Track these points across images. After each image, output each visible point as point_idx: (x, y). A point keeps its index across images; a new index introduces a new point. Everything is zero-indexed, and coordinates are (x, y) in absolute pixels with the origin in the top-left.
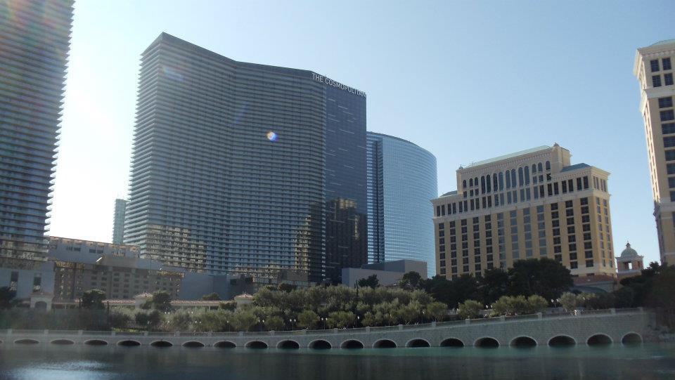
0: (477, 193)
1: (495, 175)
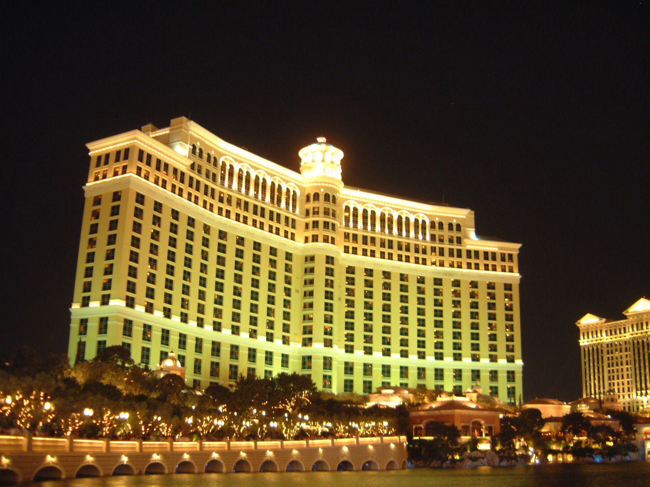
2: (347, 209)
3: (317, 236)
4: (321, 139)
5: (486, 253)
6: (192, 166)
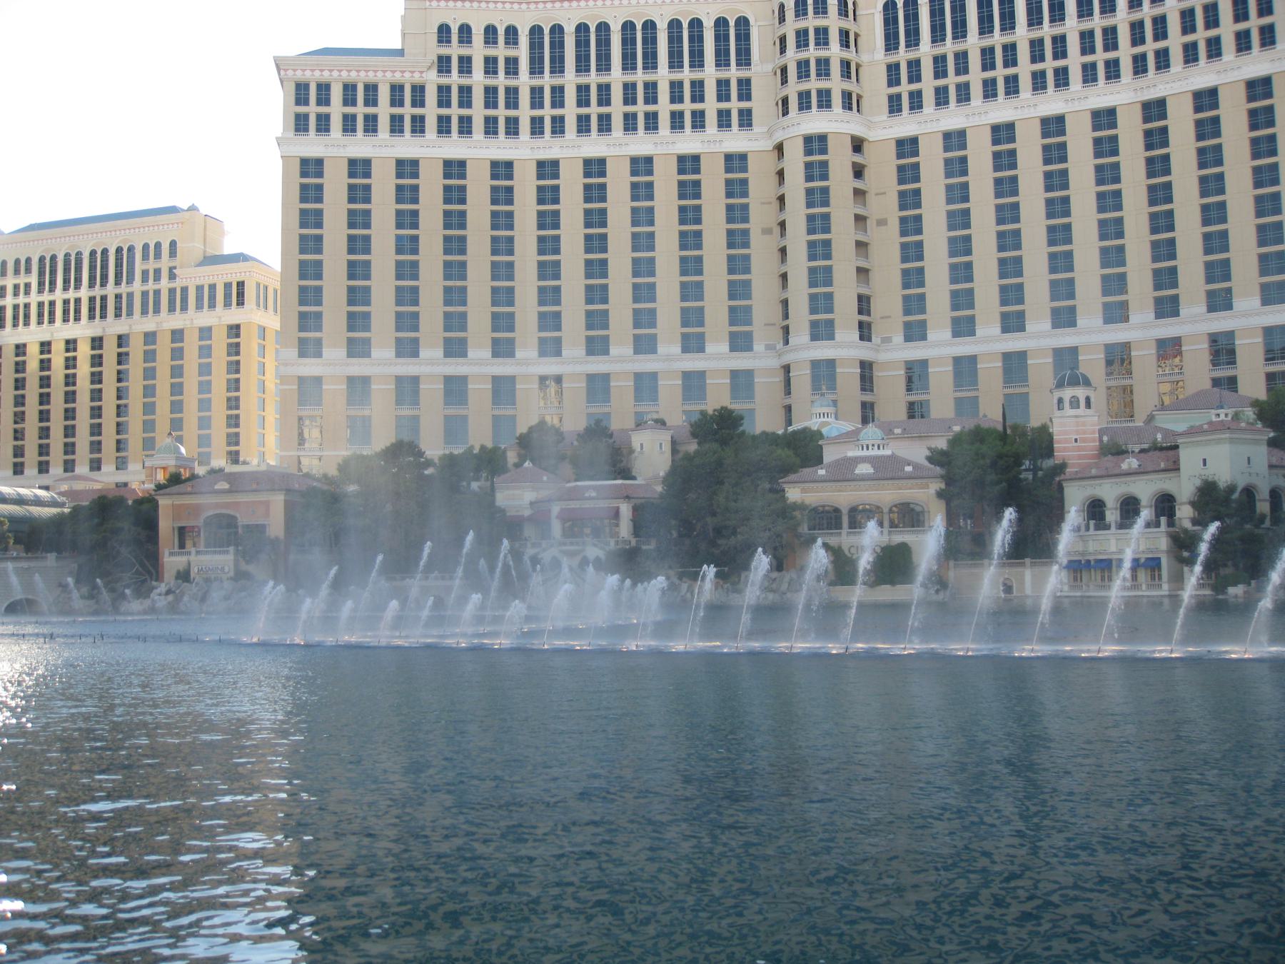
0: (27, 292)
1: (67, 255)
6: (443, 64)
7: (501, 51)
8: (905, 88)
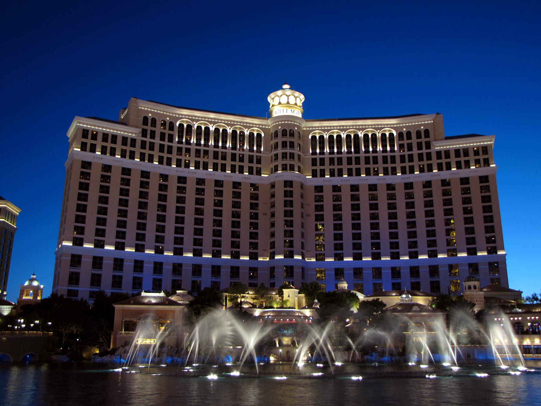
2: (314, 137)
3: (277, 165)
4: (286, 86)
5: (457, 152)
6: (144, 133)
7: (167, 132)
8: (318, 168)
